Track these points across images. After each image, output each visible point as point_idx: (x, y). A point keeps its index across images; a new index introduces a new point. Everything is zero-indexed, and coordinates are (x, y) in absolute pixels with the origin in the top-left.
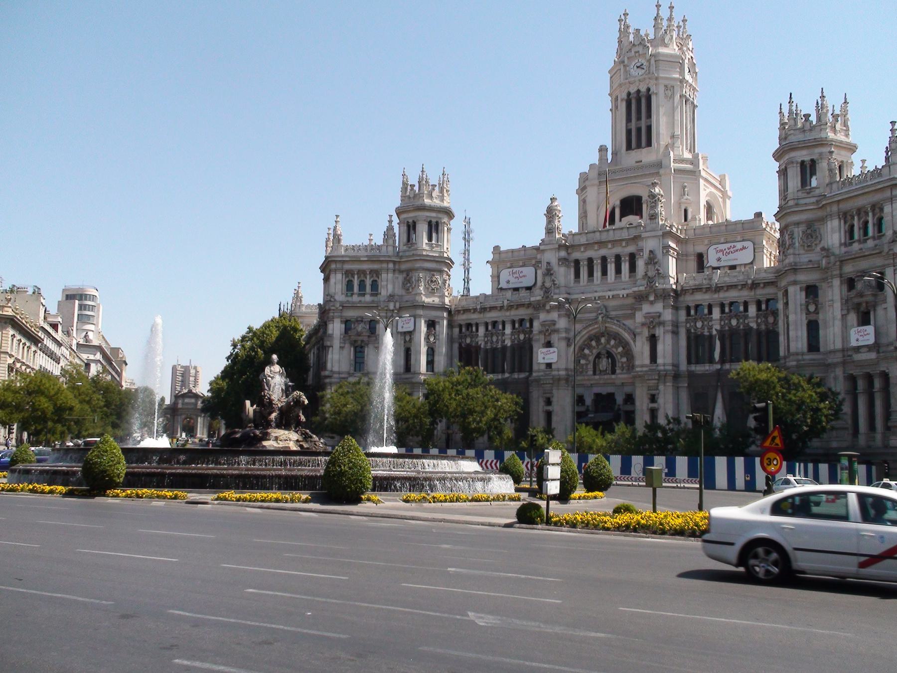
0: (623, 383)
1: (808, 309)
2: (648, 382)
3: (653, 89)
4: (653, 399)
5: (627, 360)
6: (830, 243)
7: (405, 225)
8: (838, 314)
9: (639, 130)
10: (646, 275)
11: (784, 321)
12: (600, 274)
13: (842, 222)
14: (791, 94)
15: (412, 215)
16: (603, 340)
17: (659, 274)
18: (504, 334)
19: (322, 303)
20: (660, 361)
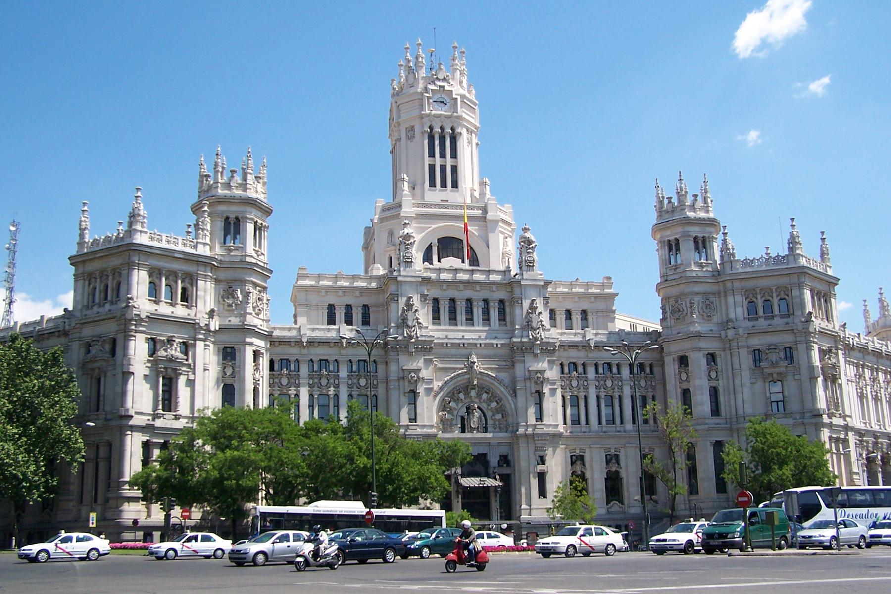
0: (499, 443)
1: (710, 376)
2: (536, 442)
3: (458, 130)
4: (542, 461)
5: (503, 417)
6: (732, 315)
7: (223, 220)
8: (747, 381)
9: (443, 168)
10: (528, 325)
11: (676, 385)
12: (464, 318)
13: (744, 298)
14: (680, 172)
15: (233, 208)
16: (473, 393)
17: (543, 325)
18: (337, 377)
19: (70, 308)
20: (546, 421)
